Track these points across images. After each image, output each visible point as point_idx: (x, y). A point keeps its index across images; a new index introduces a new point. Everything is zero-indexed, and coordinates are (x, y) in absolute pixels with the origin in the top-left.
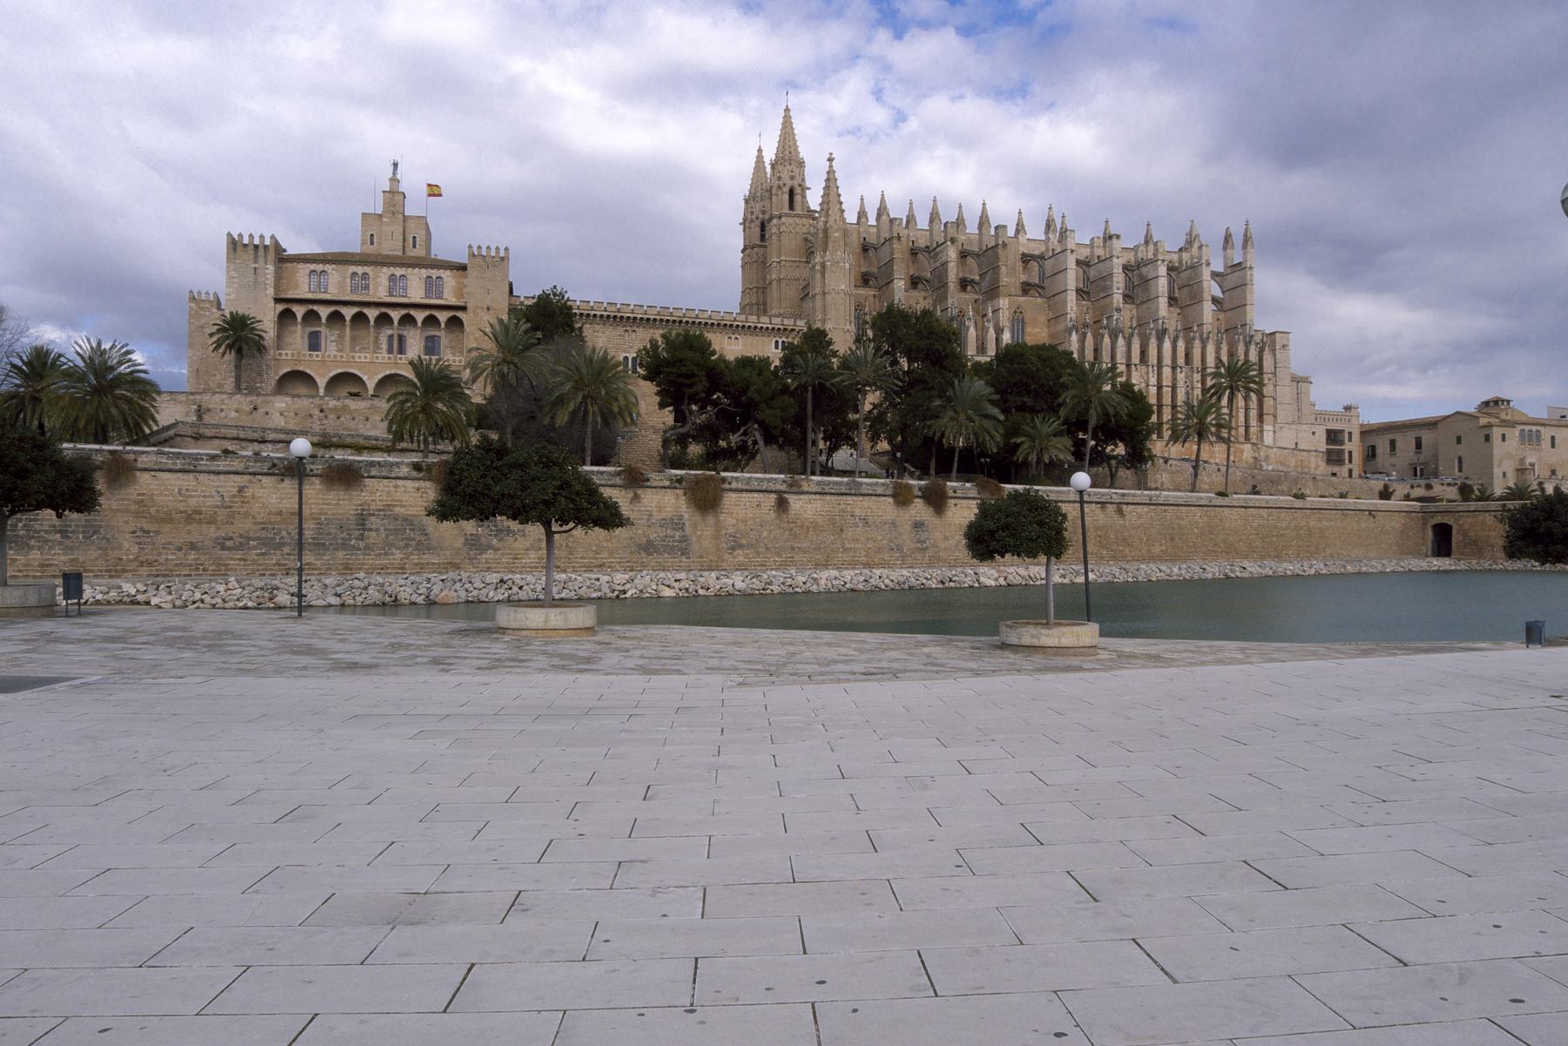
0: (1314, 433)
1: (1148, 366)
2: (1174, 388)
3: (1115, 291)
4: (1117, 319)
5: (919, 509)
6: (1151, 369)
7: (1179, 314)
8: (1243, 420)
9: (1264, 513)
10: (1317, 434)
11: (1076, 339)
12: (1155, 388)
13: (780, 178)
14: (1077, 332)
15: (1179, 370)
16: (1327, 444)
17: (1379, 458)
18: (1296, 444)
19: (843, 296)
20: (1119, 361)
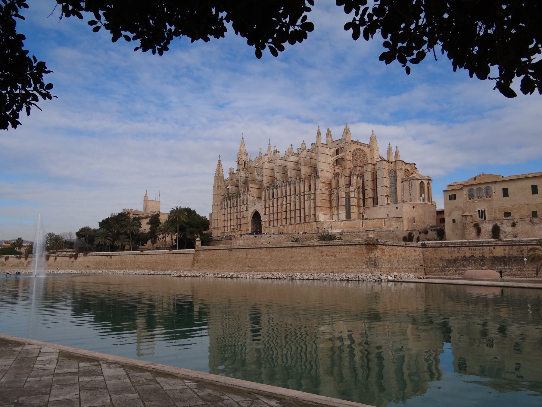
5: (73, 259)
9: (153, 256)
10: (398, 209)
18: (388, 214)
20: (274, 198)
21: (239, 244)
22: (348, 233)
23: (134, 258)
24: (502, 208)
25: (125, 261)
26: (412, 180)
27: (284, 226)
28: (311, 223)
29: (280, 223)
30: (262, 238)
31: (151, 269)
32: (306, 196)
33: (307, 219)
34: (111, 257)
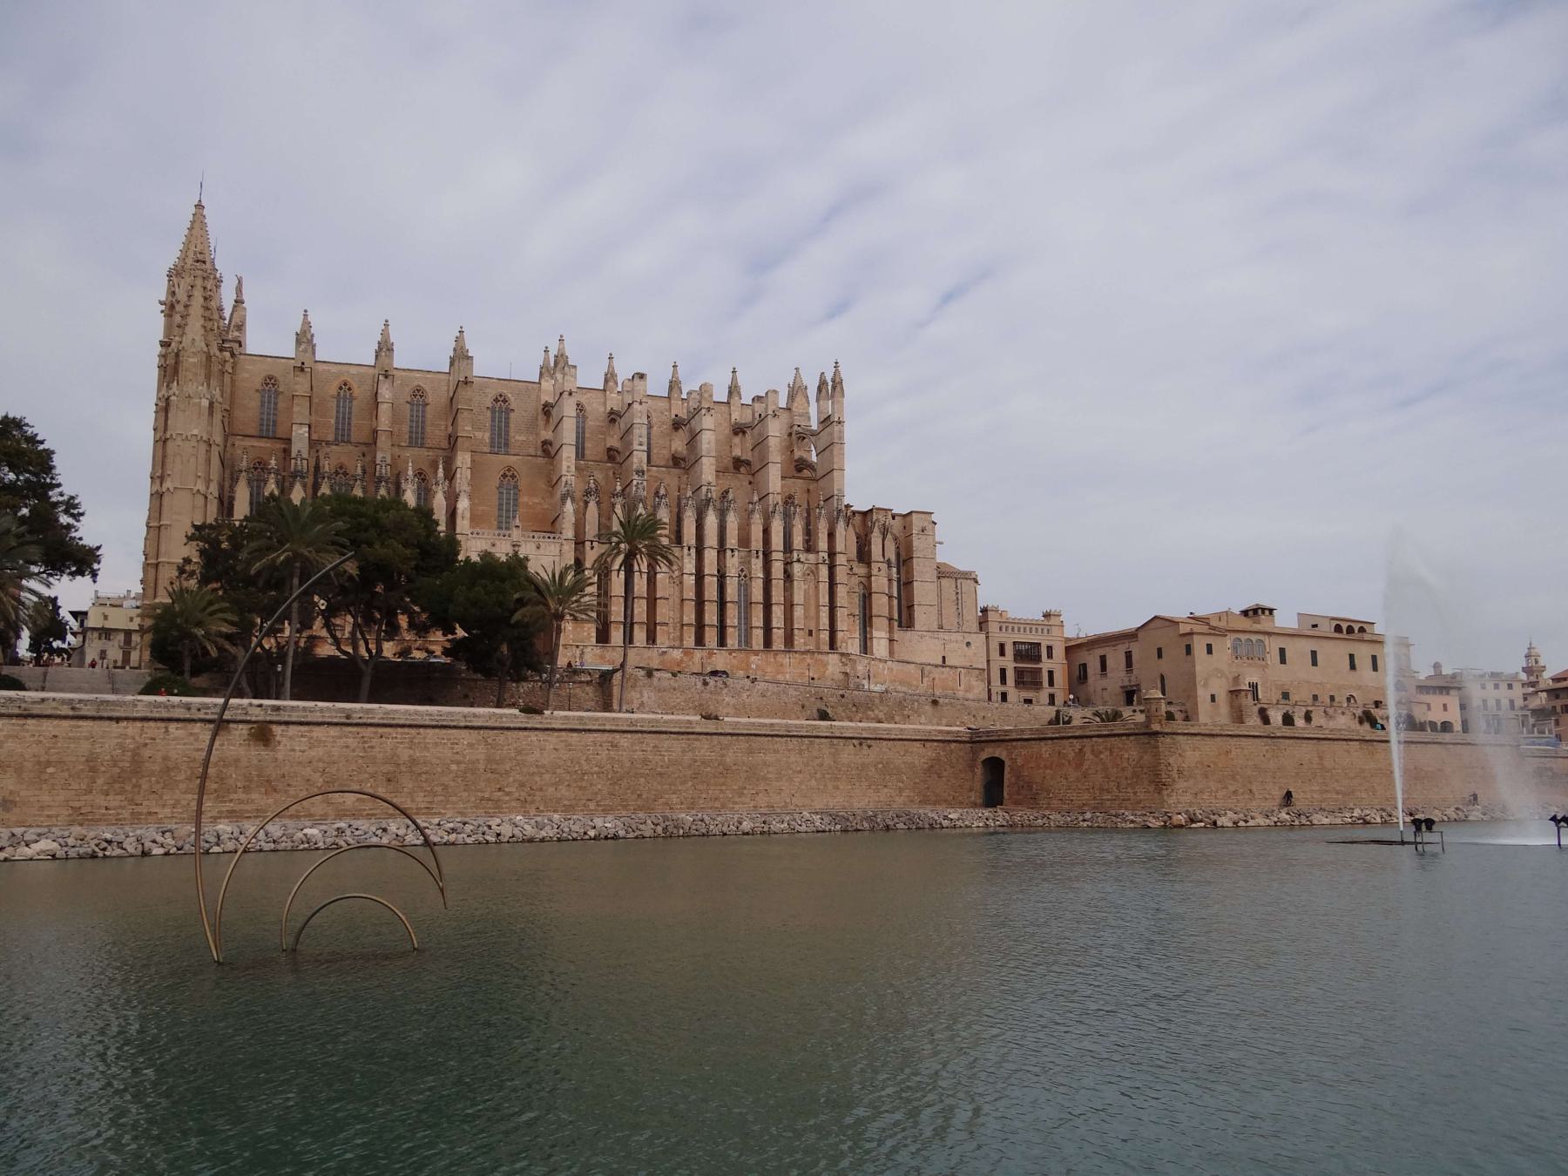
0: (968, 644)
1: (682, 547)
2: (722, 577)
3: (636, 447)
4: (636, 486)
6: (686, 550)
7: (750, 483)
8: (828, 623)
9: (624, 741)
10: (973, 647)
11: (572, 511)
12: (693, 577)
13: (174, 293)
14: (573, 500)
15: (729, 553)
16: (1015, 660)
17: (1091, 679)
18: (944, 657)
19: (196, 444)
21: (642, 704)
22: (947, 701)
23: (482, 749)
24: (1279, 683)
25: (413, 761)
26: (967, 579)
27: (687, 652)
28: (820, 656)
29: (661, 638)
30: (725, 691)
31: (625, 807)
32: (797, 568)
33: (800, 640)
34: (262, 733)
